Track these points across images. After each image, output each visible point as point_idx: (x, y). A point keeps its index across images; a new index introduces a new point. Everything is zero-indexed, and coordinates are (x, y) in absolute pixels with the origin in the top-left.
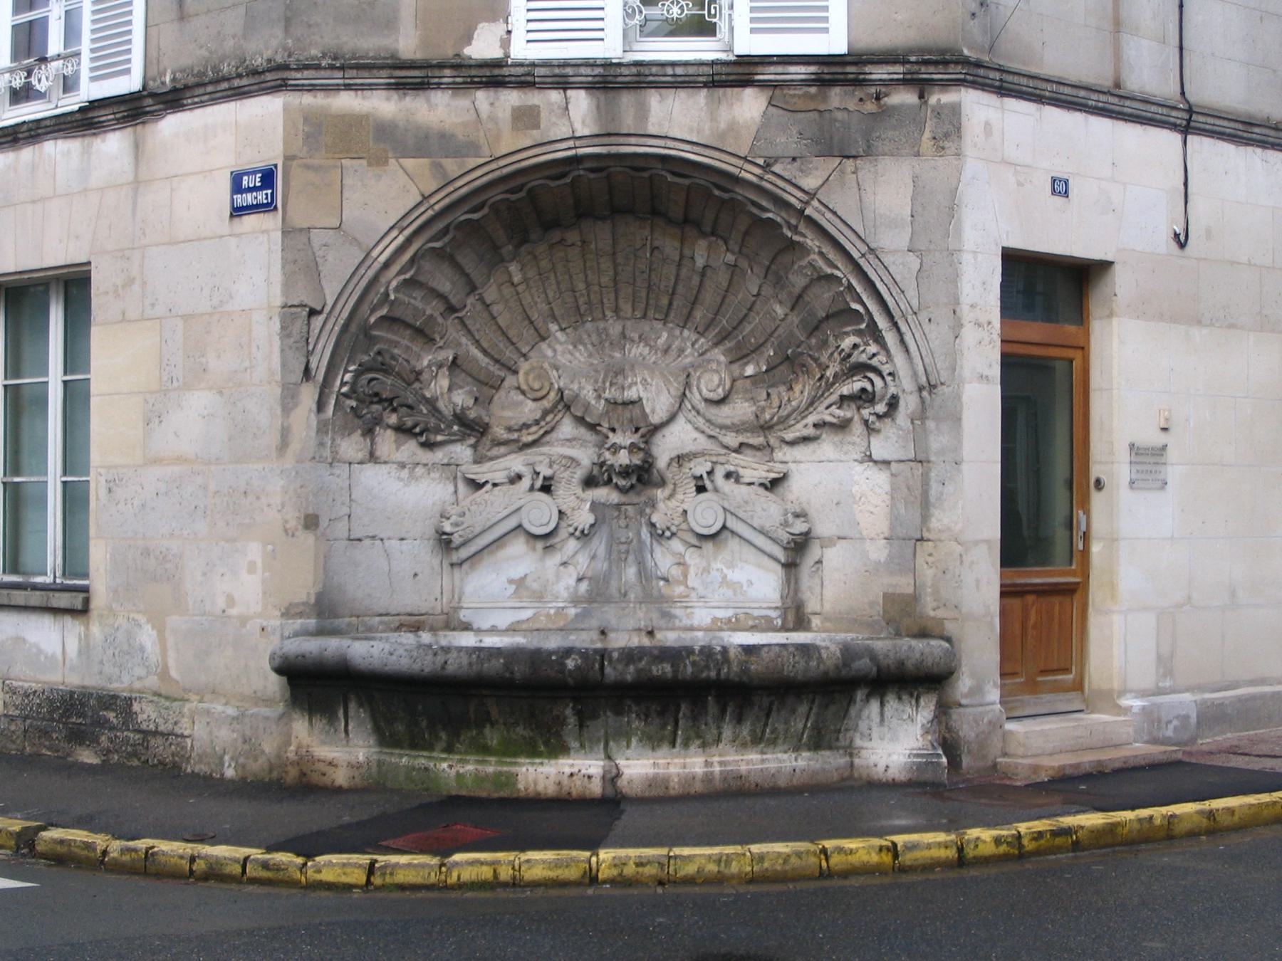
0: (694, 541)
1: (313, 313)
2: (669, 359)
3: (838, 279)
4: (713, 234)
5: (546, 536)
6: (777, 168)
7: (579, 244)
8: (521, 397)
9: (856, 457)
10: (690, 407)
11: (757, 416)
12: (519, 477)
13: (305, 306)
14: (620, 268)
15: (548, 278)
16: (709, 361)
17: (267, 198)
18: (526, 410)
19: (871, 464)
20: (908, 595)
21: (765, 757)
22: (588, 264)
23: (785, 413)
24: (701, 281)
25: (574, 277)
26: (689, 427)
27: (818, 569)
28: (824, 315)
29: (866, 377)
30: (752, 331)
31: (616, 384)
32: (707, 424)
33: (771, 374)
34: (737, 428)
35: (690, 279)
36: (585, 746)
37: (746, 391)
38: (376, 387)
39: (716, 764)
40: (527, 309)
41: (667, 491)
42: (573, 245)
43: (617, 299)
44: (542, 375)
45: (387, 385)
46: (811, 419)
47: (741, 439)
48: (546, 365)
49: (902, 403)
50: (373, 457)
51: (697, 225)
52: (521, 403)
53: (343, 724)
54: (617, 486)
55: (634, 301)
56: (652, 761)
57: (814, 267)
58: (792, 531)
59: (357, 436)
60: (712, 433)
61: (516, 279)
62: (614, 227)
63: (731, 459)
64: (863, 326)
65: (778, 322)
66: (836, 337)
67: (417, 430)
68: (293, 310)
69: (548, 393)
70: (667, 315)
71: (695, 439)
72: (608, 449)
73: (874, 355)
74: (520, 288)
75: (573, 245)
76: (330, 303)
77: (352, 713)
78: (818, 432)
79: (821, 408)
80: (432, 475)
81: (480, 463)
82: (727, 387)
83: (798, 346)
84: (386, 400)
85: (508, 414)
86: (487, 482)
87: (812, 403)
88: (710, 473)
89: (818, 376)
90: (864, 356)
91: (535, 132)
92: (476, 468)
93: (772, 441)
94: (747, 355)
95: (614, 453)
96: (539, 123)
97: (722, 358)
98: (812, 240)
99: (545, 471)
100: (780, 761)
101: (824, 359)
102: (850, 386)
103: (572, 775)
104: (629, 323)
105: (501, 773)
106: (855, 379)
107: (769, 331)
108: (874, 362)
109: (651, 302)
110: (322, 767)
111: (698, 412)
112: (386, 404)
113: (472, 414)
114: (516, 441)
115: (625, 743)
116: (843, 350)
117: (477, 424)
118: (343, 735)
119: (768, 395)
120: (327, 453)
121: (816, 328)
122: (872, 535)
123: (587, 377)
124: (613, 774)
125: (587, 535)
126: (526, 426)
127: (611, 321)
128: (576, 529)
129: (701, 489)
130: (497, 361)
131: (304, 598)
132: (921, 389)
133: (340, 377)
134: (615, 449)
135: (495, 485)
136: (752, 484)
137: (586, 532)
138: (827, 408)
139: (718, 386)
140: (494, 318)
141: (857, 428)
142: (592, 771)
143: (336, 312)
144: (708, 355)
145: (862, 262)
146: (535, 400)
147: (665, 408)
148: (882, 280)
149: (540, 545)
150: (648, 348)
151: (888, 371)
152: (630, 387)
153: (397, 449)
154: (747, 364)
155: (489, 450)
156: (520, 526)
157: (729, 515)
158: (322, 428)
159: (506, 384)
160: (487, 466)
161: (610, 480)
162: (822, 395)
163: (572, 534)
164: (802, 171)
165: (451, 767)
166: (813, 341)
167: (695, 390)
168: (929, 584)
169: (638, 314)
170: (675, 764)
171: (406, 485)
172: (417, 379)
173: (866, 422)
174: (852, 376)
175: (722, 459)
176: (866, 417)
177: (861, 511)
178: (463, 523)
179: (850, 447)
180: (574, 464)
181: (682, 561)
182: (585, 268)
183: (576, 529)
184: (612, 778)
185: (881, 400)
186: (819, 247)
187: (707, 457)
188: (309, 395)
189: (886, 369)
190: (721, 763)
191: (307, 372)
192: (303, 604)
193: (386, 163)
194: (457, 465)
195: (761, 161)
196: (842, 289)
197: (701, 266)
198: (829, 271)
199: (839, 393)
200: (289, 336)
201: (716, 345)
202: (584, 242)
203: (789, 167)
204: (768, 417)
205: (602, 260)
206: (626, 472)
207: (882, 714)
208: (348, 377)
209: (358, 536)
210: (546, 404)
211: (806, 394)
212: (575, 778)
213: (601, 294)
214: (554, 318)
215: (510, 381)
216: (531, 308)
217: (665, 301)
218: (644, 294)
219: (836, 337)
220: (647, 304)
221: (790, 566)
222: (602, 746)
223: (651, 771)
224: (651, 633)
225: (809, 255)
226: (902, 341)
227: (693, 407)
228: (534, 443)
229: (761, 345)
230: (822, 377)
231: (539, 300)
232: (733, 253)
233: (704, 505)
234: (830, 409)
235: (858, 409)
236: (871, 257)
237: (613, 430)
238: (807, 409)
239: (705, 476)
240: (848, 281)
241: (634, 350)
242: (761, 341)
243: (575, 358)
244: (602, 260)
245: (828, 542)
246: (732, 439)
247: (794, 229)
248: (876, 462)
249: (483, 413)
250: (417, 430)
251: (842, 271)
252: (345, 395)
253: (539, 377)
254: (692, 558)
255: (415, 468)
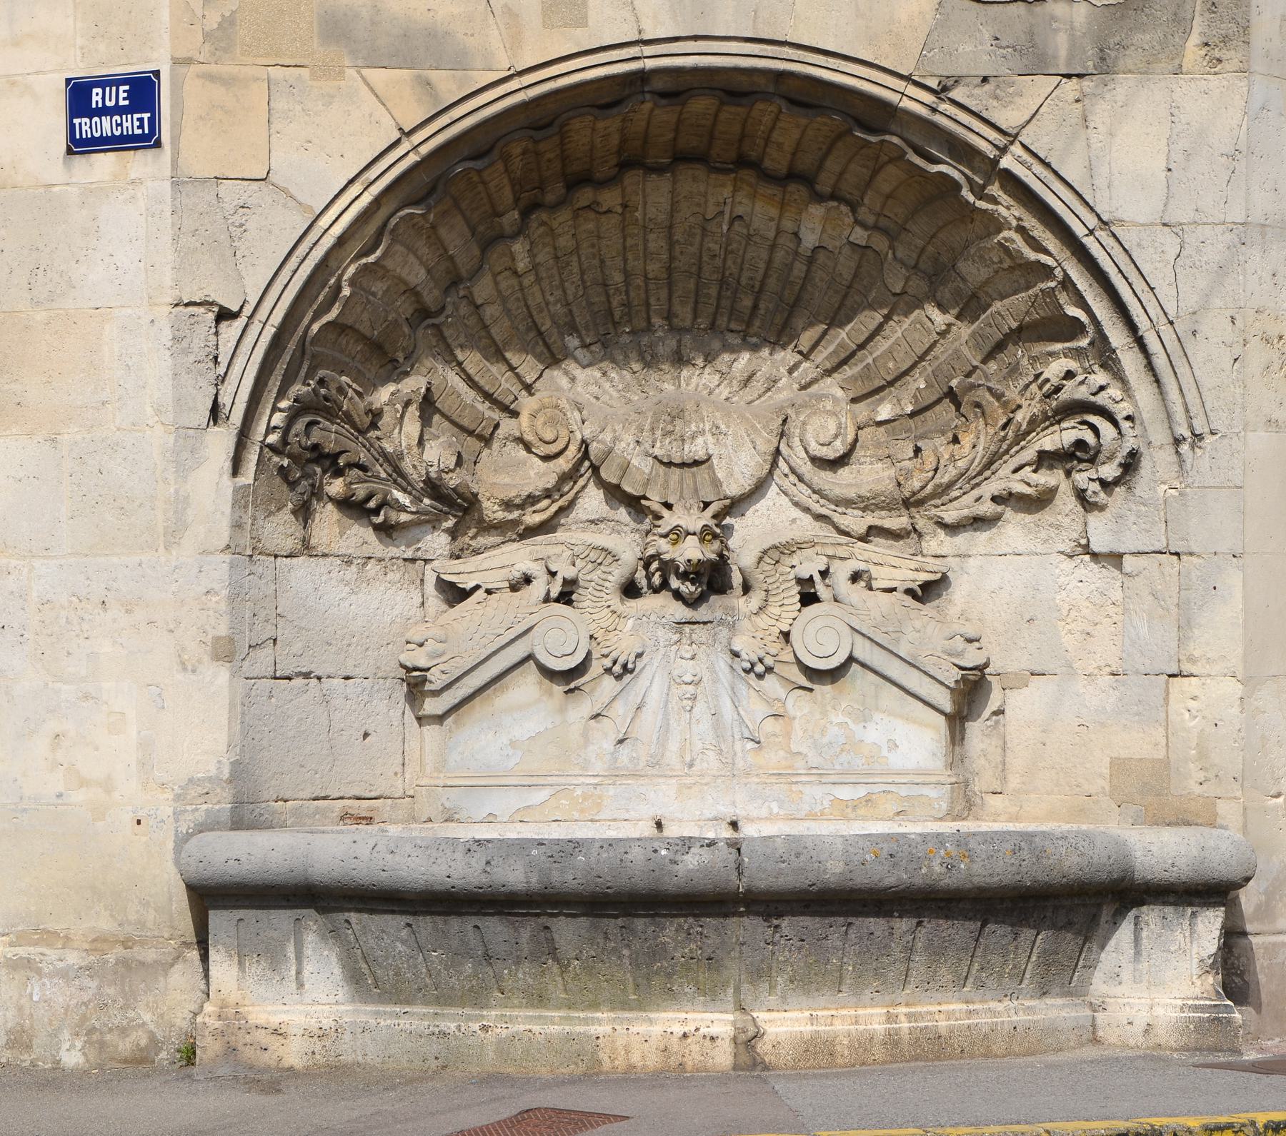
0: (803, 681)
1: (224, 315)
2: (749, 394)
3: (1047, 272)
4: (833, 197)
5: (569, 674)
6: (956, 94)
7: (620, 210)
8: (523, 453)
9: (1062, 547)
10: (787, 470)
11: (899, 485)
12: (527, 580)
13: (212, 304)
14: (677, 248)
15: (568, 264)
16: (820, 398)
17: (141, 127)
18: (532, 473)
19: (1087, 558)
20: (1160, 761)
21: (971, 1007)
22: (629, 242)
23: (946, 479)
24: (808, 271)
25: (608, 263)
26: (784, 500)
27: (997, 722)
28: (1015, 325)
29: (1084, 423)
30: (890, 351)
31: (671, 432)
32: (815, 497)
33: (919, 419)
34: (865, 504)
35: (790, 267)
36: (710, 993)
37: (878, 445)
38: (316, 436)
39: (902, 1018)
40: (534, 313)
41: (755, 600)
42: (609, 211)
43: (670, 299)
44: (556, 417)
45: (329, 435)
46: (993, 486)
47: (872, 519)
48: (564, 403)
49: (1145, 464)
50: (306, 548)
51: (808, 180)
52: (523, 463)
53: (294, 968)
54: (677, 595)
55: (696, 302)
56: (807, 1014)
57: (1006, 250)
58: (962, 664)
59: (286, 515)
60: (824, 511)
61: (521, 266)
62: (674, 182)
63: (856, 551)
64: (1084, 343)
65: (936, 337)
66: (1034, 359)
67: (372, 504)
68: (191, 309)
69: (565, 448)
70: (749, 324)
71: (794, 521)
72: (665, 536)
73: (1102, 388)
74: (526, 282)
75: (609, 211)
76: (253, 301)
77: (308, 951)
78: (999, 509)
79: (1005, 470)
80: (391, 576)
81: (458, 557)
82: (850, 438)
83: (968, 375)
84: (328, 456)
85: (504, 479)
86: (477, 587)
87: (988, 465)
88: (824, 574)
89: (1003, 420)
90: (1083, 388)
91: (578, 32)
92: (456, 565)
93: (921, 524)
94: (880, 389)
95: (675, 542)
96: (586, 17)
97: (839, 393)
98: (1008, 208)
99: (566, 571)
100: (994, 1013)
101: (1012, 394)
102: (1056, 436)
103: (685, 1036)
104: (687, 339)
105: (570, 1038)
106: (1064, 425)
107: (920, 351)
108: (1101, 399)
109: (724, 303)
110: (261, 1036)
111: (801, 479)
112: (327, 463)
113: (453, 480)
114: (515, 523)
115: (767, 984)
116: (1047, 380)
117: (460, 496)
118: (294, 985)
119: (917, 451)
120: (245, 540)
121: (999, 347)
122: (1090, 670)
123: (626, 422)
124: (751, 1034)
125: (632, 671)
126: (531, 500)
127: (660, 334)
128: (615, 662)
129: (809, 599)
130: (488, 396)
131: (213, 771)
132: (1177, 441)
133: (265, 419)
134: (677, 534)
135: (489, 592)
136: (894, 590)
137: (630, 666)
138: (1015, 471)
139: (836, 436)
140: (485, 327)
141: (1066, 501)
142: (714, 1030)
143: (262, 314)
144: (814, 389)
145: (1089, 242)
146: (546, 458)
147: (748, 472)
148: (1121, 271)
149: (558, 689)
150: (717, 377)
151: (1125, 414)
152: (693, 438)
153: (342, 534)
154: (882, 400)
155: (472, 538)
156: (530, 657)
157: (858, 638)
158: (241, 499)
159: (501, 432)
160: (472, 563)
161: (665, 585)
162: (1007, 452)
163: (608, 671)
164: (997, 98)
165: (485, 1028)
166: (993, 366)
167: (796, 442)
168: (1194, 744)
169: (703, 323)
170: (843, 1017)
171: (353, 592)
172: (374, 426)
173: (1081, 495)
174: (1059, 422)
175: (841, 552)
176: (1083, 485)
177: (1069, 632)
178: (443, 654)
179: (1053, 532)
180: (609, 559)
181: (781, 712)
182: (625, 248)
183: (615, 662)
184: (747, 1042)
185: (1110, 458)
186: (1019, 219)
187: (818, 548)
188: (221, 441)
189: (1121, 410)
190: (909, 1016)
191: (215, 410)
192: (210, 779)
193: (341, 74)
194: (426, 561)
195: (933, 83)
196: (1053, 284)
197: (811, 246)
198: (1032, 256)
199: (1037, 447)
200: (187, 351)
201: (829, 372)
202: (625, 206)
203: (977, 91)
204: (917, 484)
205: (652, 236)
206: (694, 573)
207: (1137, 940)
208: (278, 419)
209: (287, 673)
210: (563, 464)
211: (980, 448)
212: (689, 1040)
213: (647, 291)
214: (573, 328)
215: (508, 426)
216: (541, 311)
217: (747, 302)
218: (713, 291)
219: (1034, 359)
220: (718, 307)
221: (958, 720)
222: (731, 991)
223: (808, 1029)
224: (734, 825)
225: (999, 231)
226: (1150, 366)
227: (793, 471)
228: (545, 527)
229: (906, 373)
230: (1009, 421)
231: (552, 299)
232: (864, 226)
233: (819, 623)
234: (1022, 472)
235: (1068, 474)
236: (1101, 234)
237: (668, 506)
238: (980, 473)
239: (817, 578)
240: (1064, 271)
241: (694, 380)
242: (905, 367)
243: (605, 392)
244: (652, 236)
245: (1015, 682)
246: (856, 521)
247: (980, 193)
248: (1095, 556)
249: (469, 478)
250: (372, 504)
251: (1056, 254)
252: (271, 447)
253: (552, 422)
254: (798, 705)
255: (365, 564)
